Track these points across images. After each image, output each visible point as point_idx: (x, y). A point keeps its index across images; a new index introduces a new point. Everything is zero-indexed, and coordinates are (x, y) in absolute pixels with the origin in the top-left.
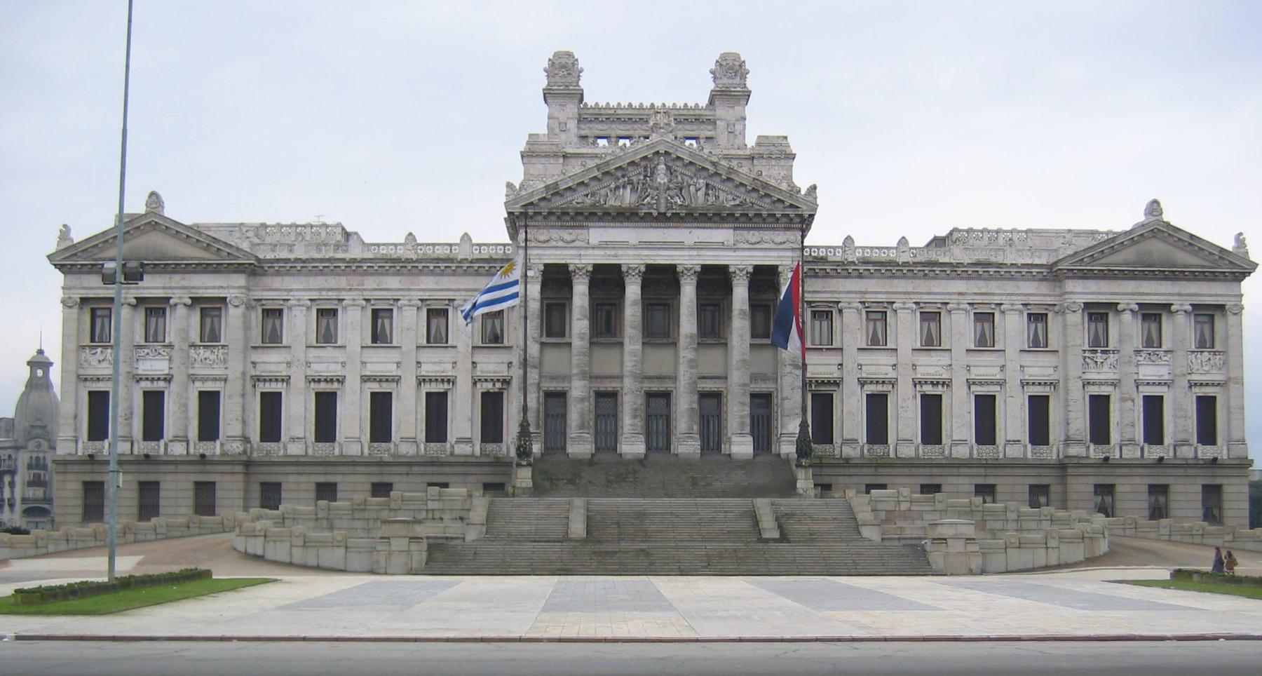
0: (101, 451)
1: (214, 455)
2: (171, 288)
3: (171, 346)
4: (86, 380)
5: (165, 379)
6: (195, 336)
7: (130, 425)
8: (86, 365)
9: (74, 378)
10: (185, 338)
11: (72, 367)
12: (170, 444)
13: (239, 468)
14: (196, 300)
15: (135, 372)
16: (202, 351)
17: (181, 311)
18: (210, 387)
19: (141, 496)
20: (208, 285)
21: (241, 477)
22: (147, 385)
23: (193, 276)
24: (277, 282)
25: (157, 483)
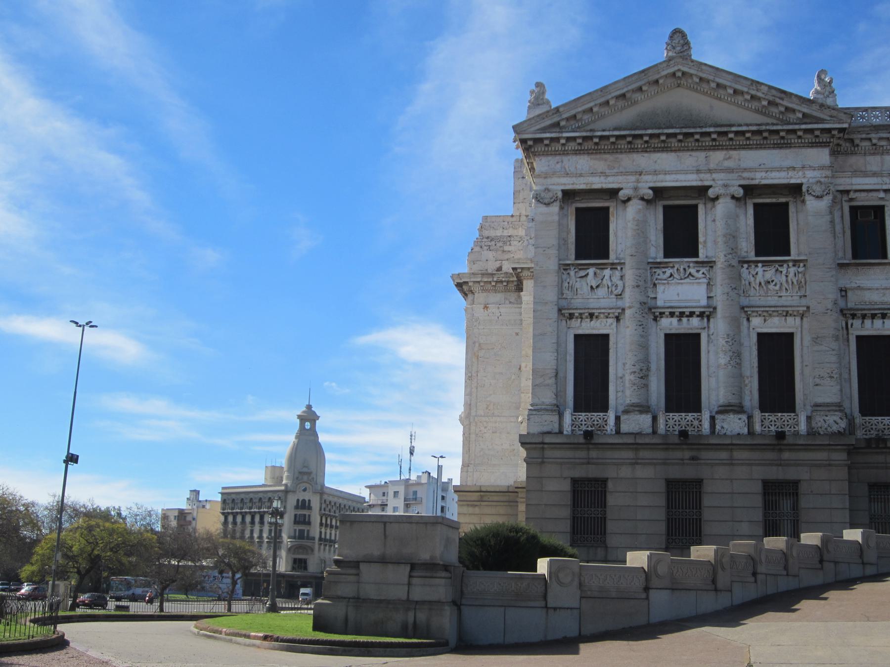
0: (601, 428)
1: (796, 434)
2: (710, 171)
3: (710, 264)
4: (571, 316)
5: (701, 315)
6: (747, 246)
7: (646, 386)
8: (568, 294)
9: (554, 314)
10: (733, 250)
11: (551, 295)
12: (719, 417)
13: (840, 456)
14: (750, 190)
15: (651, 303)
16: (760, 269)
17: (723, 207)
18: (775, 325)
19: (671, 504)
20: (771, 166)
21: (843, 473)
22: (670, 325)
23: (743, 153)
24: (873, 162)
25: (699, 482)
